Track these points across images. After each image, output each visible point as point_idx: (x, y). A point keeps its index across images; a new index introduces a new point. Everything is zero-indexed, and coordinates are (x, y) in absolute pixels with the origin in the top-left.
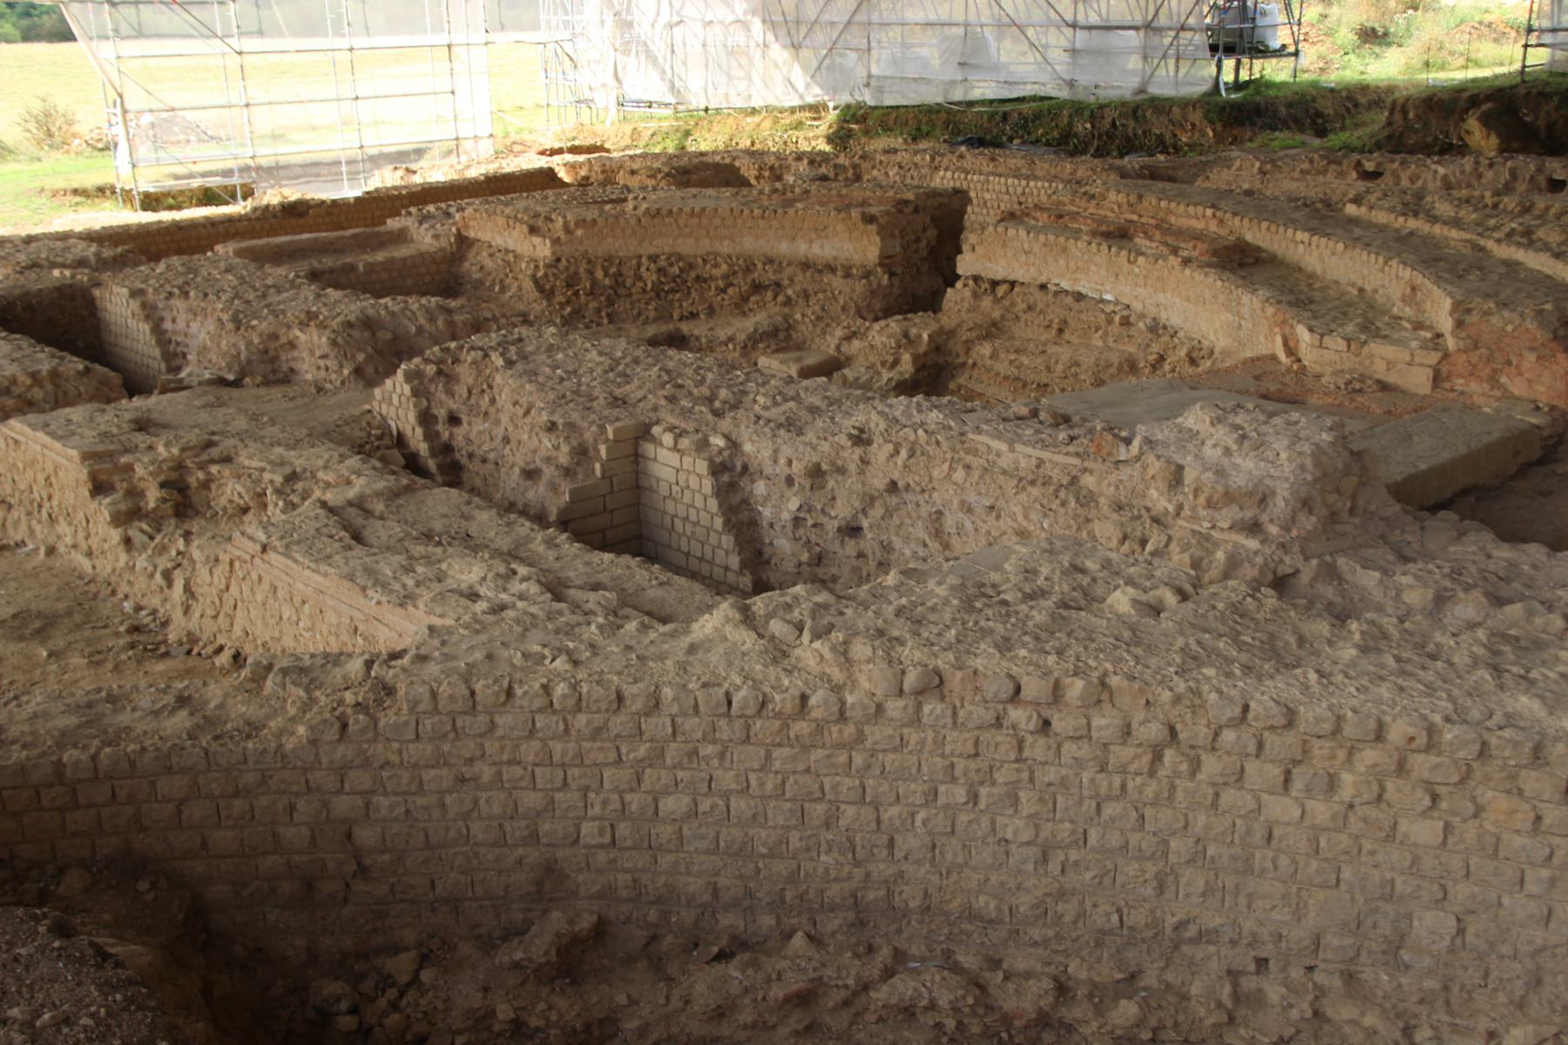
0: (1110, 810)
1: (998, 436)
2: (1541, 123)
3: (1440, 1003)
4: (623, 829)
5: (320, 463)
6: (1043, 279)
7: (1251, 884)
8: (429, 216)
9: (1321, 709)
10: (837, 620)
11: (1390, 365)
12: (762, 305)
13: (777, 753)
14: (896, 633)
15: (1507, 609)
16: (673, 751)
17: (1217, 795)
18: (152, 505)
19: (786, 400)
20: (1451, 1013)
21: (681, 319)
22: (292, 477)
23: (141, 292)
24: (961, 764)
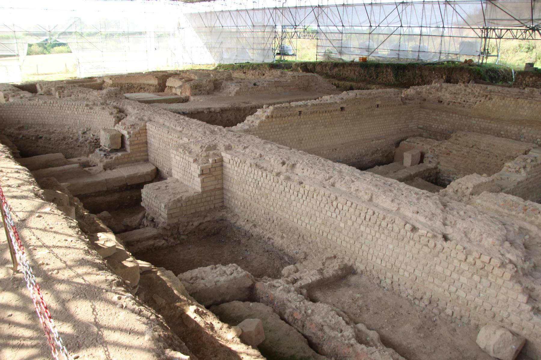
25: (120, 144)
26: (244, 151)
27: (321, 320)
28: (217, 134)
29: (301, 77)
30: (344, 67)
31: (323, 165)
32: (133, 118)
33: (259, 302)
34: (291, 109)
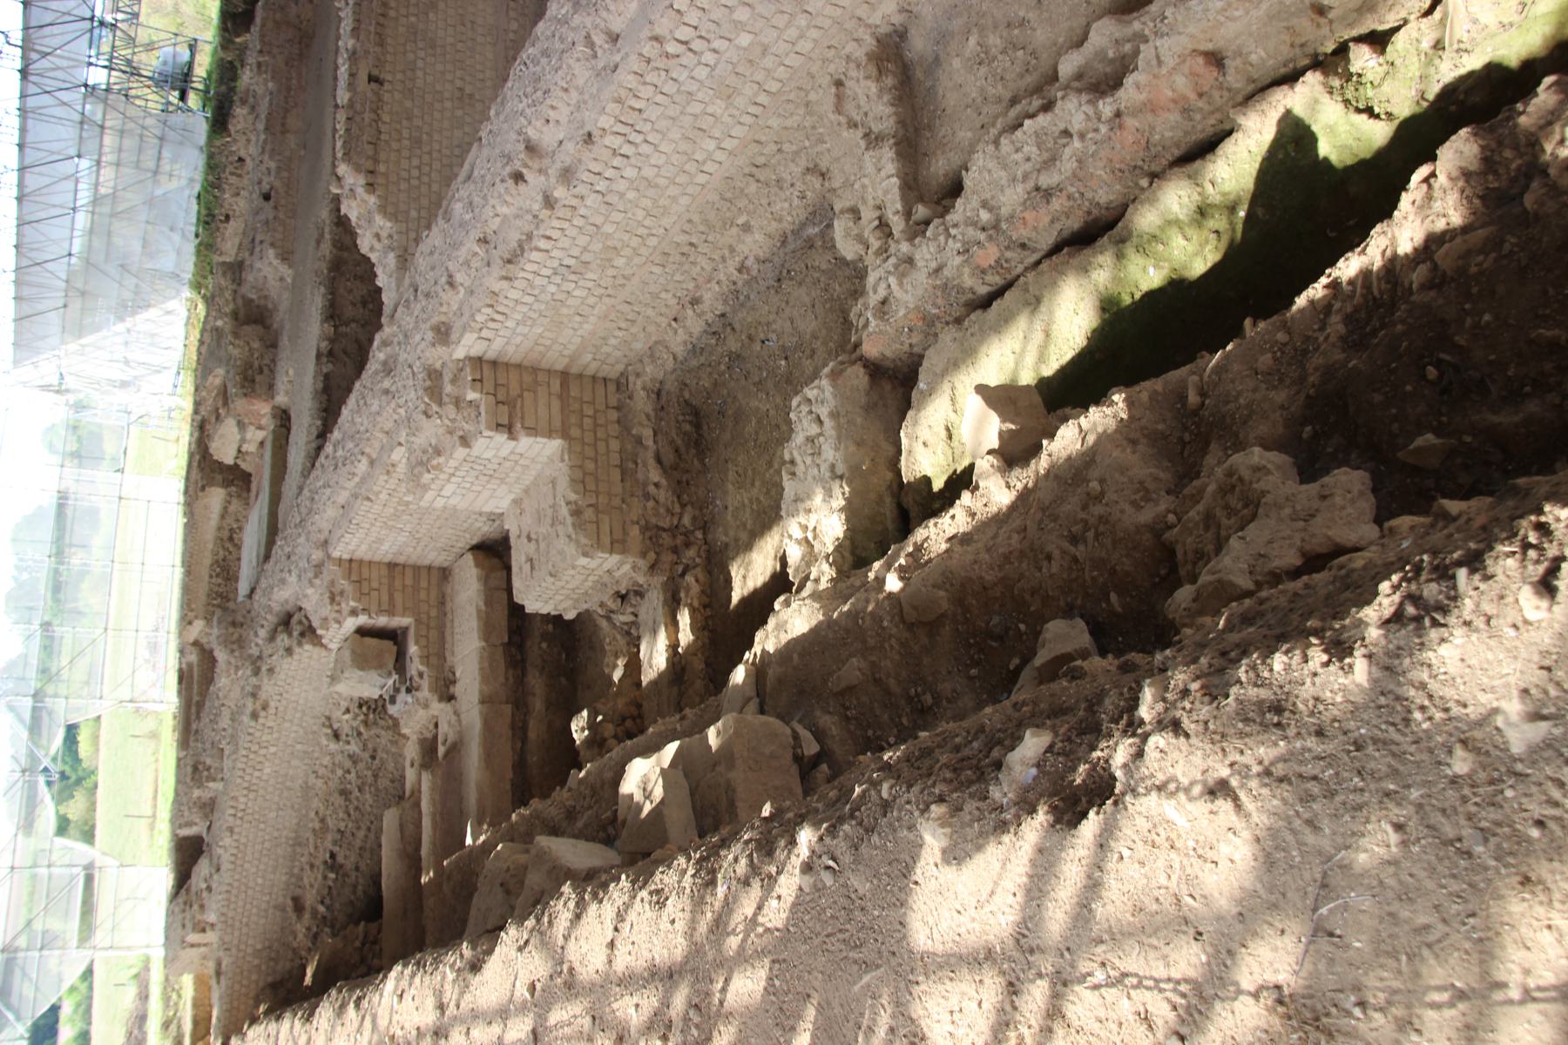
25: (381, 645)
26: (462, 291)
27: (1020, 189)
28: (395, 358)
29: (262, 42)
31: (546, 53)
32: (310, 591)
33: (922, 357)
34: (358, 107)
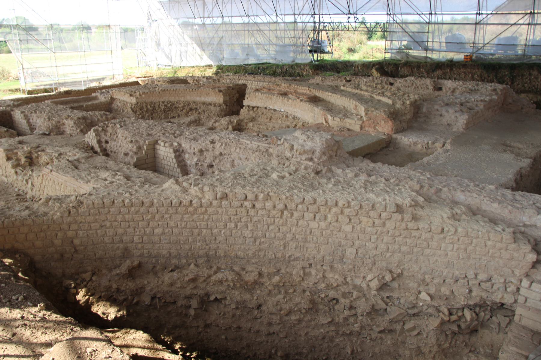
0: (271, 227)
1: (248, 140)
2: (389, 71)
3: (353, 271)
4: (145, 238)
5: (68, 151)
6: (266, 106)
7: (307, 245)
8: (103, 92)
9: (322, 199)
10: (201, 182)
11: (350, 124)
12: (192, 114)
13: (185, 216)
14: (216, 185)
15: (372, 177)
16: (157, 217)
17: (298, 222)
18: (23, 163)
19: (194, 133)
20: (355, 273)
21: (171, 118)
22: (60, 154)
23: (24, 112)
24: (232, 217)
30: (451, 70)
